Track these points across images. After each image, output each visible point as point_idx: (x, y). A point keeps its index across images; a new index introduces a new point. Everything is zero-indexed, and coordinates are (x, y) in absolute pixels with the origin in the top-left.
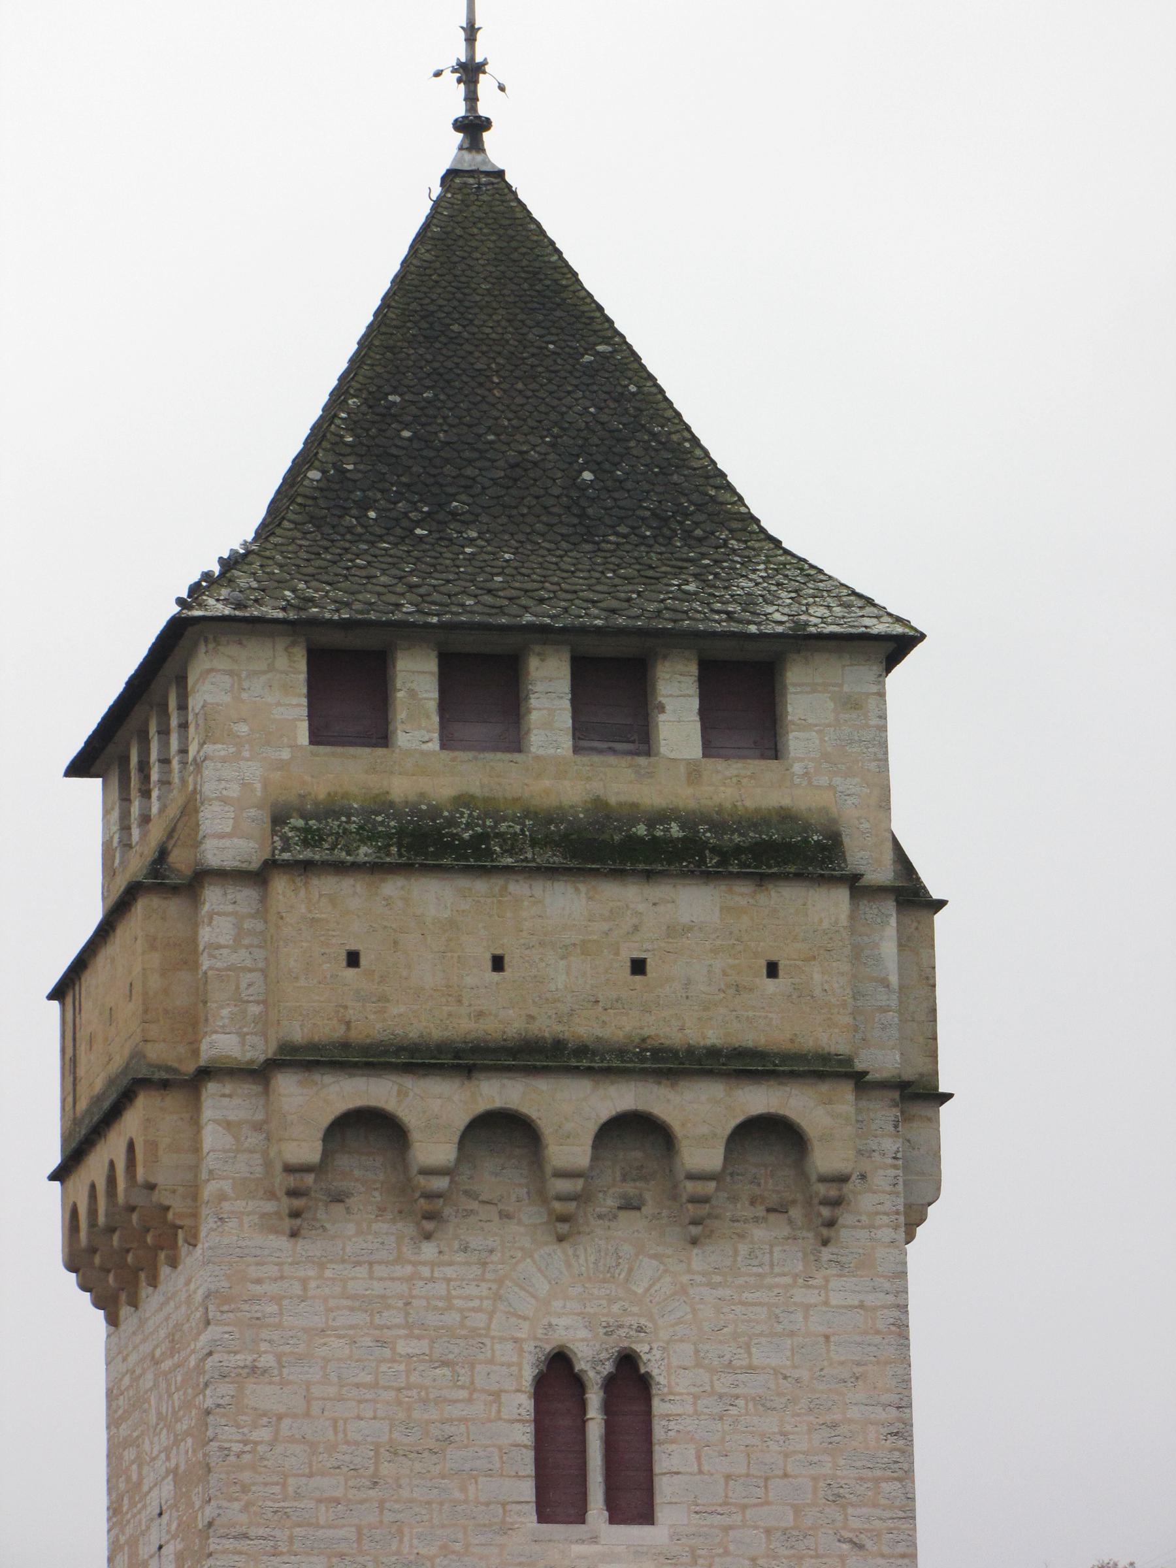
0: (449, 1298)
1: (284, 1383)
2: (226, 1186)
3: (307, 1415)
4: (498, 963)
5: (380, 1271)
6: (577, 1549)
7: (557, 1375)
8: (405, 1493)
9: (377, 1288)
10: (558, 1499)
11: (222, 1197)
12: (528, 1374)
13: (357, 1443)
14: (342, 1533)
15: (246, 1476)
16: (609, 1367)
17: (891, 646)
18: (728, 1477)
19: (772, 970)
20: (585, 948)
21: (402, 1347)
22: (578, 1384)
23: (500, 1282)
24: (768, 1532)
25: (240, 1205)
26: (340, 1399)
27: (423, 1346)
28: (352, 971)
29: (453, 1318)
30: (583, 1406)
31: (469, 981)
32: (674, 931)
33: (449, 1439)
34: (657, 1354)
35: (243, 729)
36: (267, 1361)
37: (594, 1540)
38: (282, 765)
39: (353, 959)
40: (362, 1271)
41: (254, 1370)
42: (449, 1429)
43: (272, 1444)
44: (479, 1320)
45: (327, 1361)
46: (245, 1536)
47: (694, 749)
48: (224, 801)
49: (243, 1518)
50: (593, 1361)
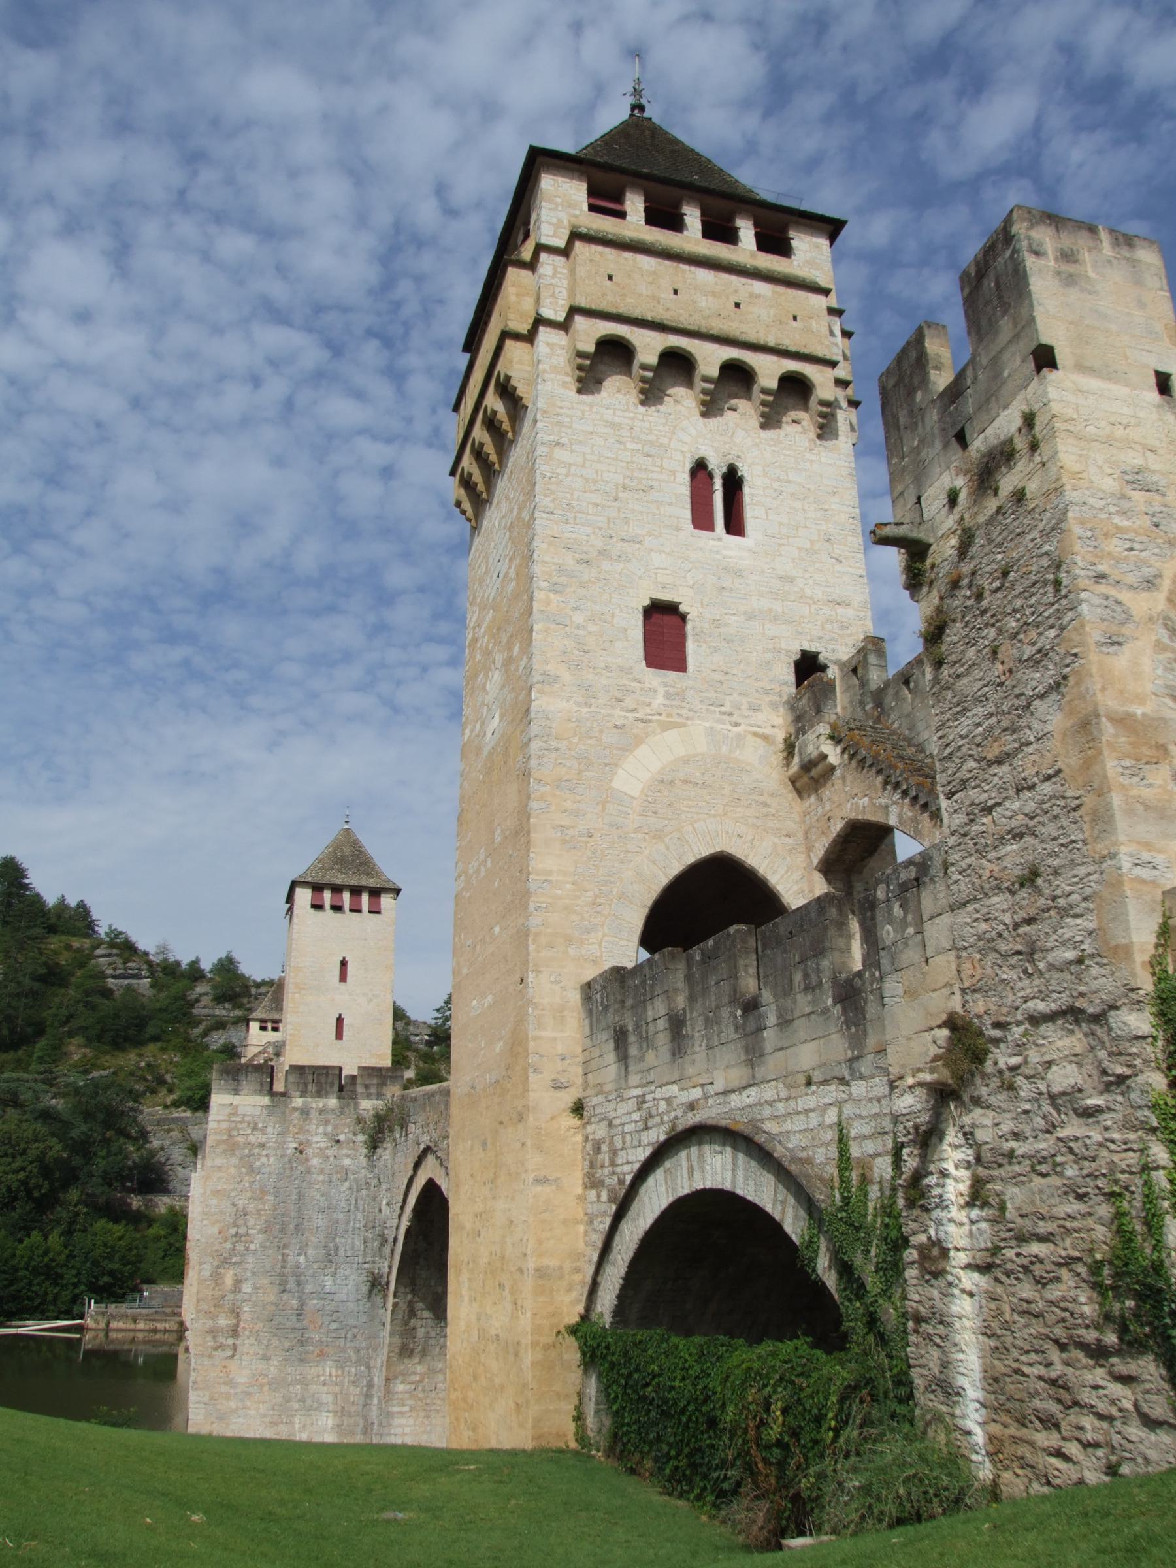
0: (651, 430)
1: (572, 451)
2: (547, 367)
3: (583, 466)
4: (676, 292)
5: (618, 413)
6: (712, 542)
7: (700, 469)
8: (630, 506)
9: (617, 420)
10: (702, 519)
11: (545, 371)
12: (688, 466)
13: (608, 482)
14: (601, 518)
15: (553, 487)
16: (724, 470)
17: (830, 228)
18: (780, 524)
19: (795, 318)
20: (714, 294)
21: (630, 446)
22: (711, 476)
23: (675, 427)
24: (799, 549)
25: (553, 376)
26: (599, 462)
27: (639, 447)
28: (609, 282)
29: (652, 438)
30: (712, 485)
31: (663, 296)
32: (751, 295)
33: (651, 487)
34: (746, 468)
35: (559, 200)
36: (564, 440)
37: (720, 540)
38: (576, 216)
39: (610, 278)
40: (610, 412)
41: (558, 444)
42: (651, 483)
43: (567, 476)
44: (666, 441)
45: (593, 445)
46: (552, 513)
47: (755, 248)
48: (550, 224)
49: (551, 505)
50: (717, 468)
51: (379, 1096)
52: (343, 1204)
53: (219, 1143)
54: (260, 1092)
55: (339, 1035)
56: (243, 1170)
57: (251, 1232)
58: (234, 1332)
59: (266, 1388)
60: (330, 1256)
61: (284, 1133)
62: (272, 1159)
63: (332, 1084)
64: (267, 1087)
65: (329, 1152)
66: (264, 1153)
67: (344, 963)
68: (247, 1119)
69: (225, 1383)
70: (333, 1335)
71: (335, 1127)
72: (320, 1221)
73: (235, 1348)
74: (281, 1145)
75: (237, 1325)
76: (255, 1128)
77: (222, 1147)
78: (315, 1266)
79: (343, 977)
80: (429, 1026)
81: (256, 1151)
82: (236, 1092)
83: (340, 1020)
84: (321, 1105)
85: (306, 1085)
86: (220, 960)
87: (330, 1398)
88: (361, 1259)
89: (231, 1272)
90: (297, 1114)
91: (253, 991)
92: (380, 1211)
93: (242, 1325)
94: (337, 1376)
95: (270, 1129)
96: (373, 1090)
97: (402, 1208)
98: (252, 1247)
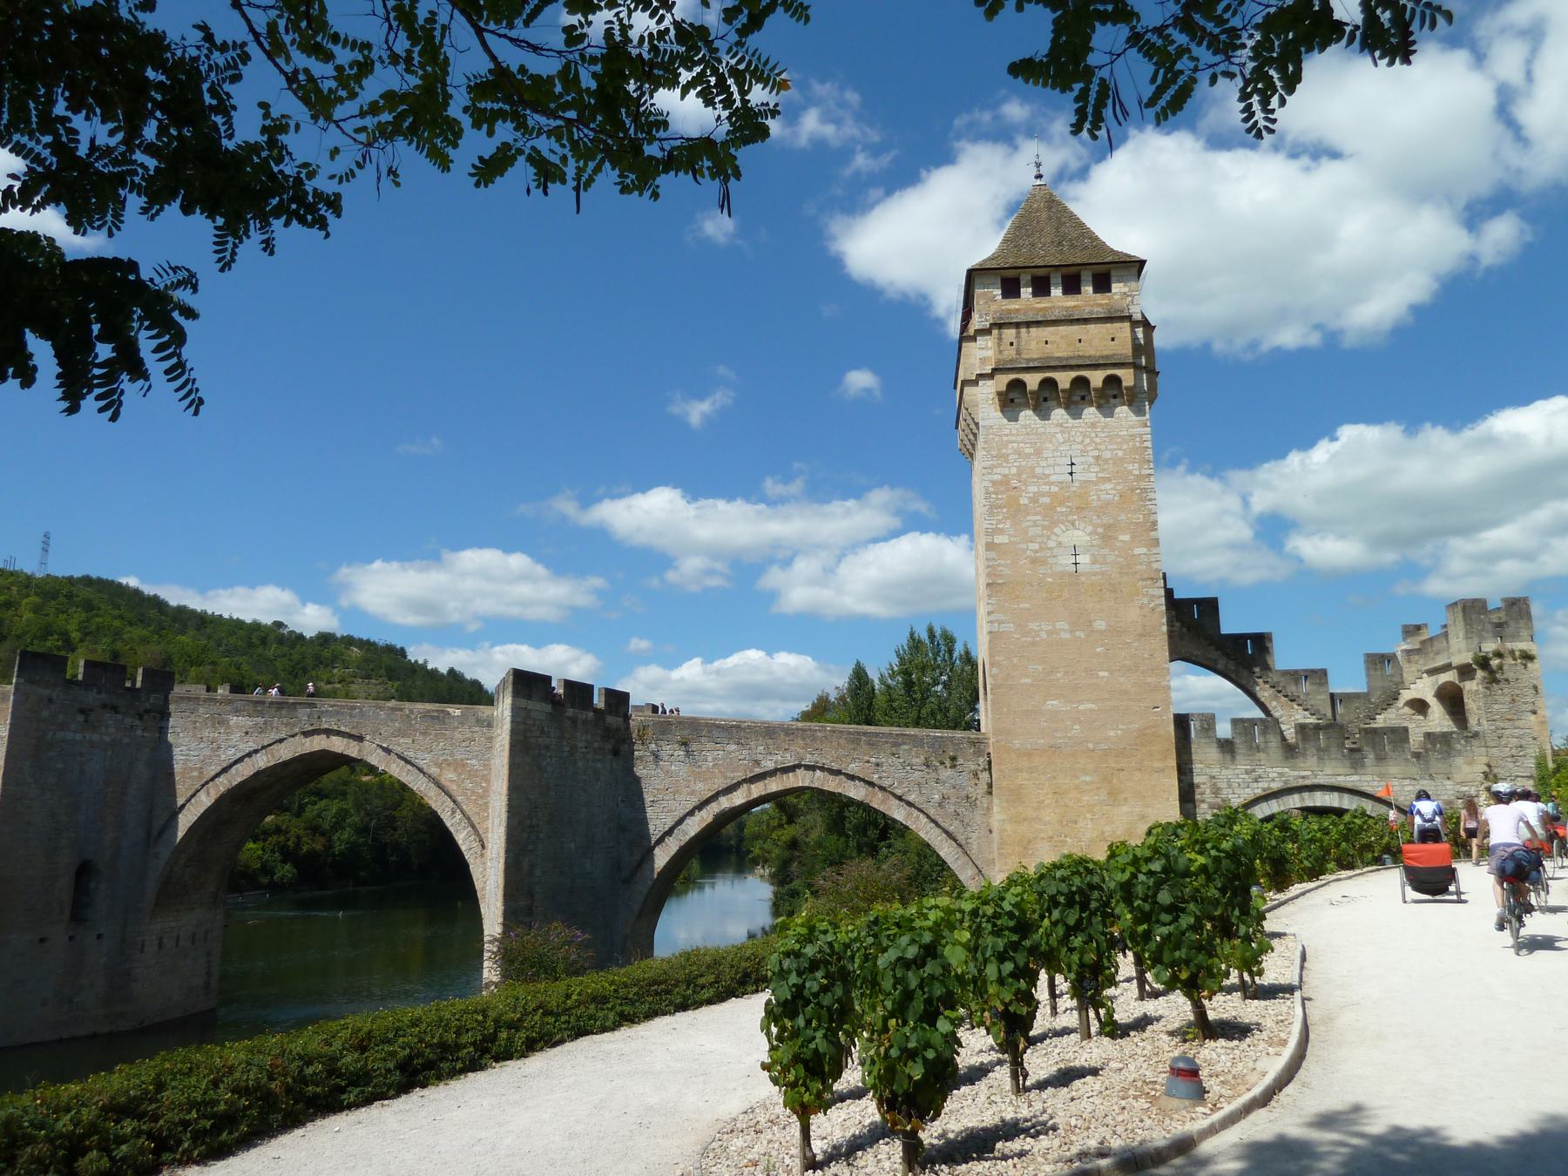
76: (542, 732)
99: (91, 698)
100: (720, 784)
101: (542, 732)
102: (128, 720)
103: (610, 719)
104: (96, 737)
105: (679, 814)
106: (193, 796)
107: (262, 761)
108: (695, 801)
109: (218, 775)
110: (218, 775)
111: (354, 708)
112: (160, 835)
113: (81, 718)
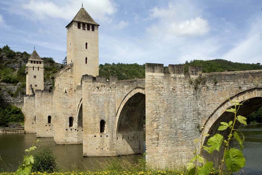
51: (196, 74)
52: (187, 104)
53: (150, 87)
54: (161, 72)
55: (86, 63)
56: (157, 95)
57: (161, 112)
58: (158, 139)
59: (167, 153)
60: (184, 119)
61: (169, 84)
62: (166, 92)
63: (182, 71)
64: (163, 71)
65: (183, 90)
66: (163, 90)
67: (86, 44)
68: (157, 80)
69: (156, 153)
70: (185, 139)
71: (184, 83)
72: (181, 109)
73: (158, 143)
74: (168, 88)
75: (159, 137)
76: (160, 83)
77: (150, 89)
78: (180, 121)
79: (86, 48)
80: (61, 64)
81: (161, 89)
82: (154, 72)
83: (86, 59)
84: (179, 76)
85: (175, 71)
86: (5, 47)
87: (185, 155)
88: (192, 119)
89: (156, 123)
90: (172, 79)
91: (16, 55)
92: (197, 106)
93: (160, 137)
94: (187, 149)
95: (165, 83)
96: (194, 73)
97: (224, 104)
98: (161, 116)
99: (99, 84)
100: (228, 97)
101: (160, 82)
102: (108, 89)
103: (192, 76)
104: (101, 93)
105: (215, 109)
106: (120, 105)
107: (130, 96)
108: (220, 103)
109: (123, 100)
110: (123, 100)
111: (143, 81)
112: (117, 114)
113: (97, 89)
